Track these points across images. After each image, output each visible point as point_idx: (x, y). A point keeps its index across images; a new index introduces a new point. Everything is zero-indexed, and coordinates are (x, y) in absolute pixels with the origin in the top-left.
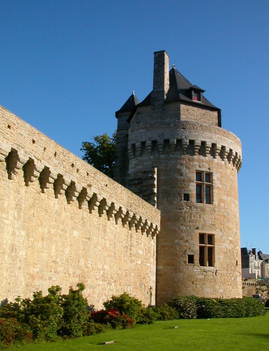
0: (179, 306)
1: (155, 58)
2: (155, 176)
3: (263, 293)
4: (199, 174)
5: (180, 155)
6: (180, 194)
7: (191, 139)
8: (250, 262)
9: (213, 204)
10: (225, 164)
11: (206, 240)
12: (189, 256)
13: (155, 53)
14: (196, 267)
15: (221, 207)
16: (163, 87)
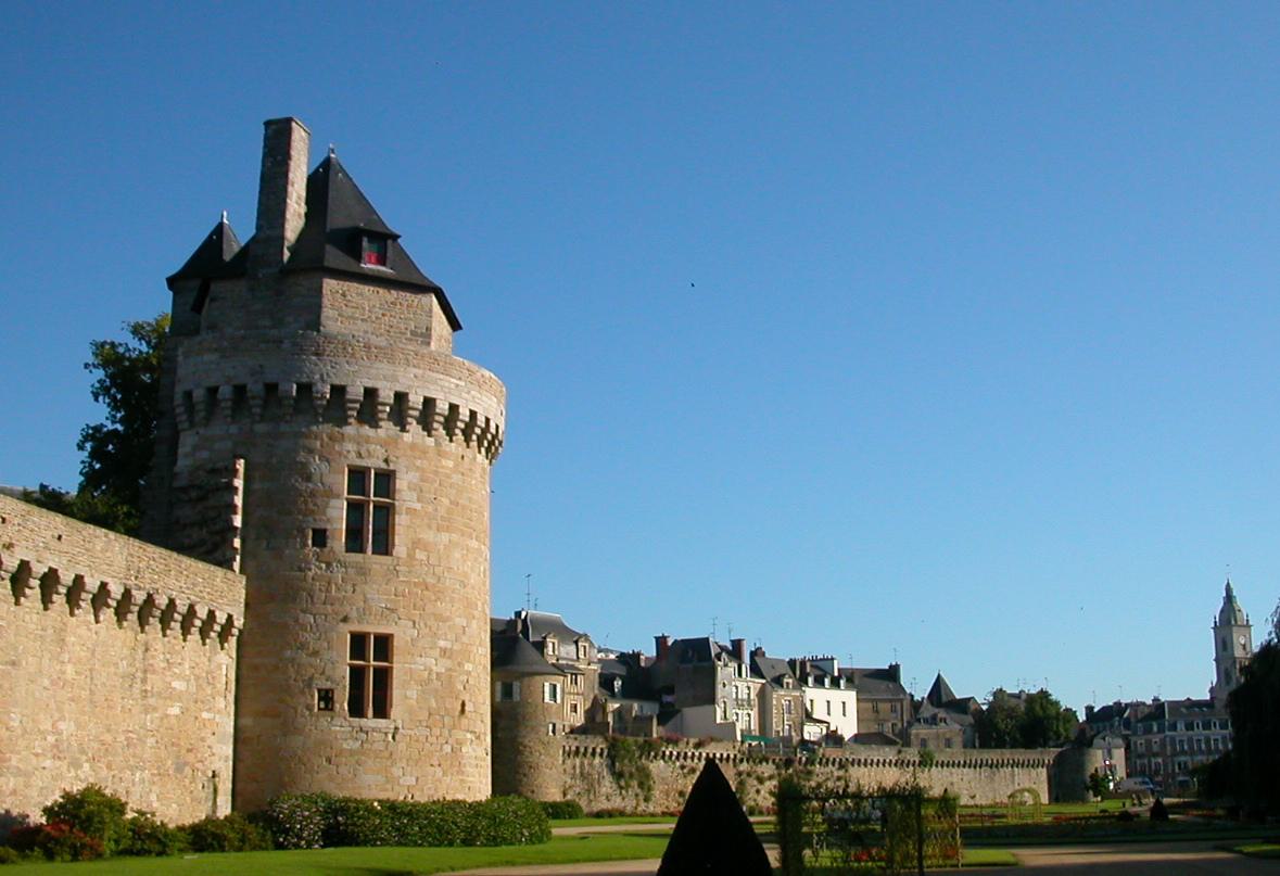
1: (266, 138)
2: (239, 483)
3: (760, 787)
4: (358, 476)
5: (308, 427)
7: (337, 382)
8: (720, 686)
9: (391, 555)
10: (438, 444)
13: (268, 124)
14: (337, 721)
15: (415, 563)
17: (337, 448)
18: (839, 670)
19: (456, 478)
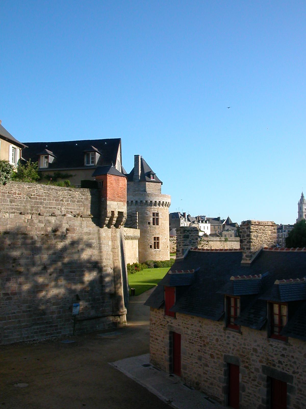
0: (148, 264)
2: (137, 216)
4: (154, 214)
5: (147, 207)
6: (146, 222)
7: (151, 200)
8: (181, 224)
9: (159, 225)
10: (164, 208)
11: (156, 239)
12: (150, 246)
13: (135, 156)
14: (153, 250)
16: (139, 173)
17: (151, 210)
18: (207, 218)
19: (166, 212)
